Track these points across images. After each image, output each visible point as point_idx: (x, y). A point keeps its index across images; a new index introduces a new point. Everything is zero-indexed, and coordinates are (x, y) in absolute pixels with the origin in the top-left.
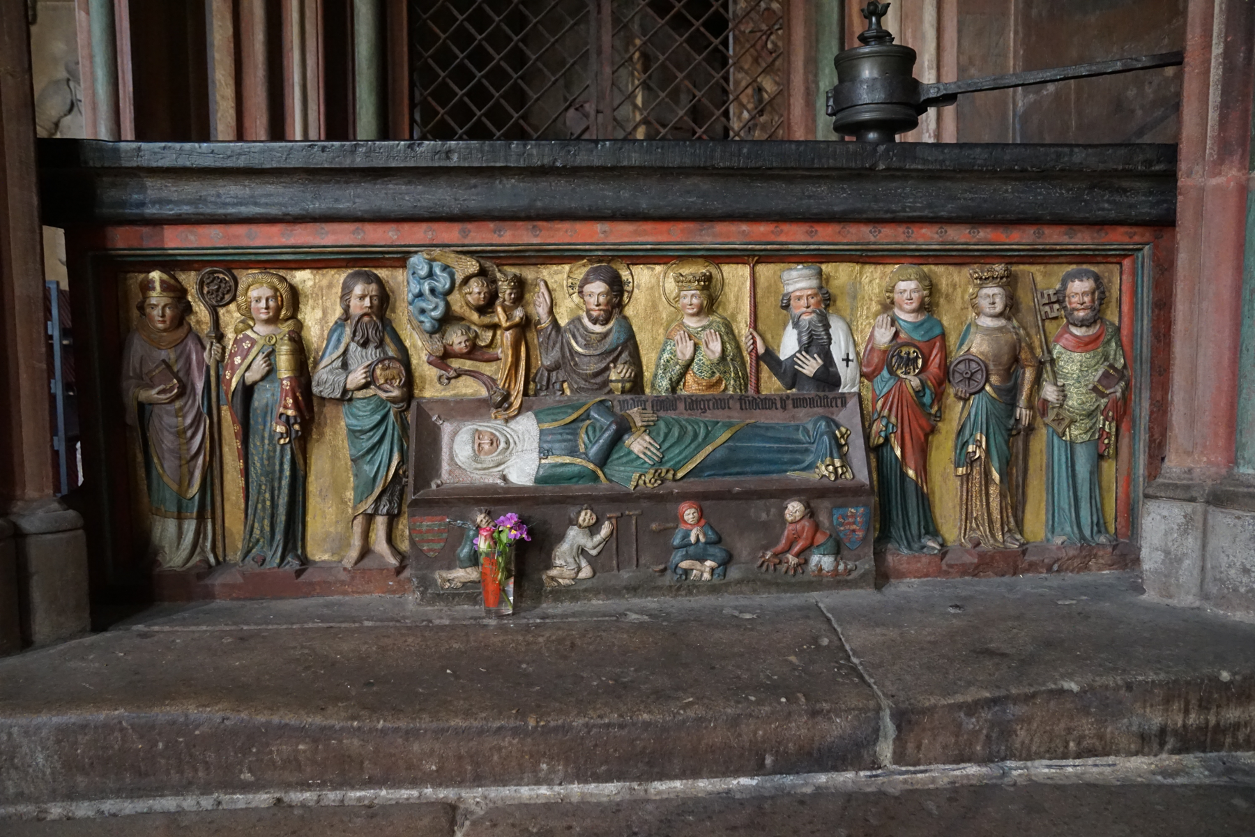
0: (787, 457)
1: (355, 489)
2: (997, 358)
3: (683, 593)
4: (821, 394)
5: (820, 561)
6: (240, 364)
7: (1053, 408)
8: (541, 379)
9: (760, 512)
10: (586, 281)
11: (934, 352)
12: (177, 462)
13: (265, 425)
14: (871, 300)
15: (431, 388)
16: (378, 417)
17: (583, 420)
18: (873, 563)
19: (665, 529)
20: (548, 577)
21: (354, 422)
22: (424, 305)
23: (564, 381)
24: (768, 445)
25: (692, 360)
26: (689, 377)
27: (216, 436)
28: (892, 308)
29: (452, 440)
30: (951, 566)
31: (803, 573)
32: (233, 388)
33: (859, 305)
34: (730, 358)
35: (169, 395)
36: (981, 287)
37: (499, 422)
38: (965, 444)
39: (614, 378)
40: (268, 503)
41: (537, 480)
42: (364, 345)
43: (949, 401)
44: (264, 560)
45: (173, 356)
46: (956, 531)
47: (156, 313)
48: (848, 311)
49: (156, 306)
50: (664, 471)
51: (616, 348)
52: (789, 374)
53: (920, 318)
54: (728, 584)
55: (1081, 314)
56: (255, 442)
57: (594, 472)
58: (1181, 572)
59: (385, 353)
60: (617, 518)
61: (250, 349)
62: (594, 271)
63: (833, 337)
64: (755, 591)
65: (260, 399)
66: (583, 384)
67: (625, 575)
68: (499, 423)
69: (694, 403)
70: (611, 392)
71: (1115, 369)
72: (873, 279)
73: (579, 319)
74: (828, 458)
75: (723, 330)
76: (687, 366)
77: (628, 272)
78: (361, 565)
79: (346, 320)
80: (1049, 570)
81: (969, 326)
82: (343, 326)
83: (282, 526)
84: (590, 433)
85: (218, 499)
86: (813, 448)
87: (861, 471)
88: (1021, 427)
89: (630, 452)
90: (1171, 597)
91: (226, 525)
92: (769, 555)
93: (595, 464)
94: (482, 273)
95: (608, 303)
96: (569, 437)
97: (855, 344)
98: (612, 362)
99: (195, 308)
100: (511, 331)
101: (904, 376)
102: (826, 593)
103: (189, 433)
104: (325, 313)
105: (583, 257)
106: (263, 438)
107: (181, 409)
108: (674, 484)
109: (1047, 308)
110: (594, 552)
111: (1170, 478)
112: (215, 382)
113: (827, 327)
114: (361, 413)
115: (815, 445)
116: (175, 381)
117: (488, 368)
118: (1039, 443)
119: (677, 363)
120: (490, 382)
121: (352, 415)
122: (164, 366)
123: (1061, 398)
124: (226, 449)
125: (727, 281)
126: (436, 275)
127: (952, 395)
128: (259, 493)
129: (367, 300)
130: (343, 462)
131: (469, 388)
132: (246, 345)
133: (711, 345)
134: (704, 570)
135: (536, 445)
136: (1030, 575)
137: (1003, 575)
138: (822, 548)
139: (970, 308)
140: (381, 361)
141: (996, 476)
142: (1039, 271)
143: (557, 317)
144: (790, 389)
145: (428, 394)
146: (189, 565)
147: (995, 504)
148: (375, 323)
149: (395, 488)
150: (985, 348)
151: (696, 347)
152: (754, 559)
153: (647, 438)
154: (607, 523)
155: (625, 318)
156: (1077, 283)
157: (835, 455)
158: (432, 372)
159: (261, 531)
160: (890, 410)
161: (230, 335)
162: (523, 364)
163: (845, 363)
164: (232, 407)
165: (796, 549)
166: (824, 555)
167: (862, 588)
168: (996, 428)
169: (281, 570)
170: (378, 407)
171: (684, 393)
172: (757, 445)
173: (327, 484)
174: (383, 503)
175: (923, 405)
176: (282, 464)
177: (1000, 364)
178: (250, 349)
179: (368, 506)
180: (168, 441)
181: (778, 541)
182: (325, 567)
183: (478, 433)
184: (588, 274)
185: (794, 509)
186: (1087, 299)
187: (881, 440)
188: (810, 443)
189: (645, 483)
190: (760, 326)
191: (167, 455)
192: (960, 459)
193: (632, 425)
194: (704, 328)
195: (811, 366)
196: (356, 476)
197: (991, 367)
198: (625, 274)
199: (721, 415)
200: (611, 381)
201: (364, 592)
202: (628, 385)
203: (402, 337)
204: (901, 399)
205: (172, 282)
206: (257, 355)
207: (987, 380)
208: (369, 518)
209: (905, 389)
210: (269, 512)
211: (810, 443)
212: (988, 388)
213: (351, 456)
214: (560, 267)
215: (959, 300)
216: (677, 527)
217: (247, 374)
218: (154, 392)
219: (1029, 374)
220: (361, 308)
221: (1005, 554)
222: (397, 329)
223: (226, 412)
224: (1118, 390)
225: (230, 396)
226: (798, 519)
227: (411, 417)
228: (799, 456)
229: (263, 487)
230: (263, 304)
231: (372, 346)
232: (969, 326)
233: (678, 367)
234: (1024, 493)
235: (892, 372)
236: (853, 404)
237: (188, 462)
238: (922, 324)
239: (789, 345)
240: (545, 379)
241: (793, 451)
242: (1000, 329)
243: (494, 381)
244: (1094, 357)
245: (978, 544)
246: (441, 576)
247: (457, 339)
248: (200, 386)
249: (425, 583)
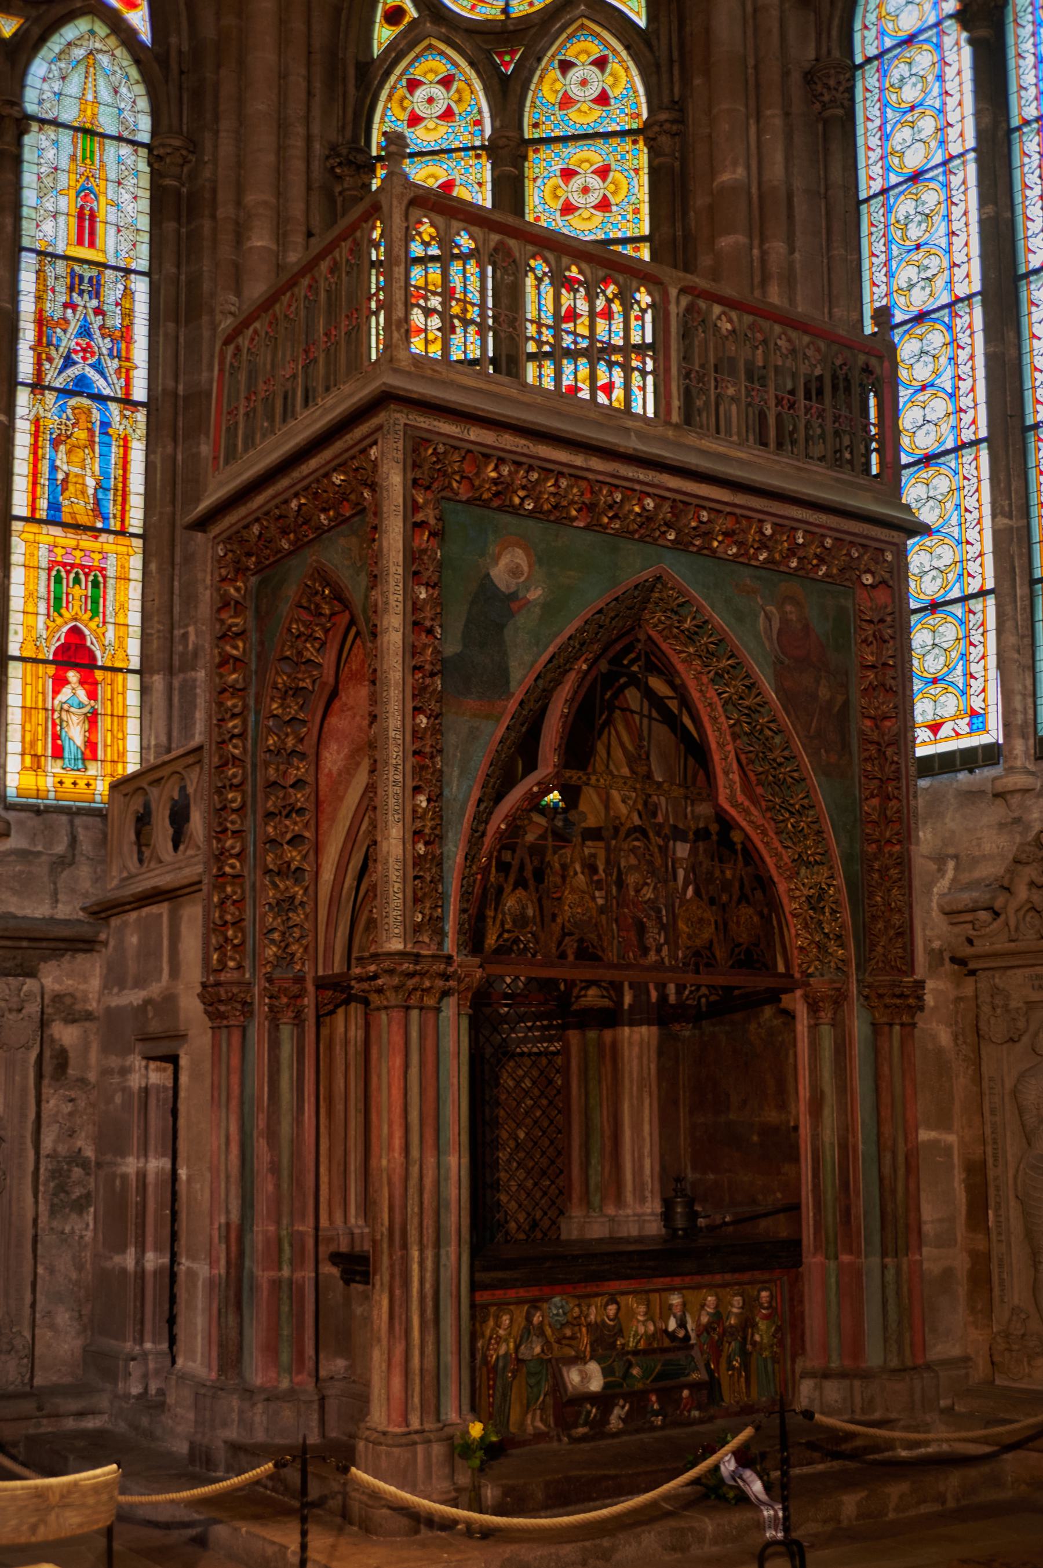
10: (607, 1304)
52: (672, 1336)
134: (659, 1420)
158: (556, 1346)
185: (686, 1393)
239: (672, 1325)
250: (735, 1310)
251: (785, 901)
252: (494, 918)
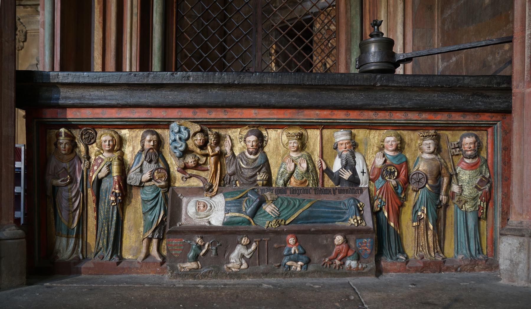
0: (335, 215)
1: (144, 227)
2: (431, 172)
3: (288, 276)
4: (351, 188)
5: (350, 263)
6: (97, 170)
7: (457, 195)
8: (227, 179)
9: (323, 240)
10: (247, 136)
11: (403, 169)
12: (68, 213)
13: (106, 197)
14: (374, 146)
16: (155, 194)
17: (245, 197)
18: (374, 265)
19: (281, 247)
20: (228, 267)
21: (144, 196)
22: (176, 145)
23: (237, 180)
24: (327, 210)
25: (294, 171)
26: (292, 179)
27: (85, 201)
28: (383, 150)
29: (187, 205)
30: (410, 268)
31: (343, 268)
32: (93, 180)
33: (369, 148)
34: (310, 170)
35: (65, 183)
36: (423, 140)
37: (207, 198)
38: (417, 211)
39: (259, 179)
40: (106, 232)
41: (224, 224)
42: (150, 162)
43: (409, 192)
44: (103, 257)
45: (68, 165)
46: (413, 252)
47: (62, 146)
48: (364, 151)
49: (62, 143)
50: (280, 220)
51: (260, 166)
52: (337, 179)
53: (396, 154)
54: (308, 273)
55: (469, 153)
56: (101, 204)
57: (249, 220)
58: (518, 270)
59: (159, 166)
60: (259, 241)
61: (101, 163)
62: (251, 131)
63: (357, 162)
64: (321, 276)
65: (105, 185)
66: (245, 181)
67: (262, 267)
68: (207, 198)
69: (294, 191)
70: (257, 185)
71: (485, 178)
73: (244, 153)
74: (354, 216)
75: (307, 158)
76: (292, 174)
77: (266, 132)
78: (145, 261)
79: (143, 151)
80: (456, 270)
81: (418, 158)
82: (141, 154)
83: (112, 242)
84: (248, 203)
85: (85, 230)
86: (347, 212)
87: (369, 222)
88: (442, 204)
89: (265, 212)
90: (514, 282)
91: (88, 241)
92: (327, 260)
93: (249, 217)
94: (202, 131)
95: (257, 145)
96: (238, 204)
97: (367, 166)
98: (258, 172)
99: (79, 145)
100: (214, 157)
101: (389, 180)
102: (353, 278)
103: (74, 200)
104: (134, 148)
105: (245, 125)
106: (105, 203)
107: (71, 189)
108: (285, 226)
109: (454, 150)
110: (248, 257)
111: (512, 226)
112: (85, 177)
113: (354, 157)
114: (148, 193)
115: (348, 211)
116: (68, 176)
117: (203, 174)
118: (451, 212)
119: (287, 173)
120: (204, 180)
121: (143, 193)
122: (64, 170)
123: (461, 191)
124: (89, 207)
125: (309, 137)
126: (182, 132)
127: (411, 189)
128: (102, 227)
129: (152, 142)
130: (139, 215)
131: (195, 182)
132: (99, 161)
133: (302, 165)
134: (298, 266)
135: (223, 208)
136: (447, 273)
137: (434, 272)
138: (351, 257)
139: (419, 150)
140: (157, 169)
141: (431, 226)
142: (450, 133)
143: (234, 152)
144: (338, 185)
145: (177, 185)
146: (71, 258)
147: (431, 239)
148: (155, 152)
150: (425, 168)
151: (296, 166)
152: (320, 262)
153: (273, 205)
154: (254, 243)
155: (264, 152)
156: (467, 138)
157: (357, 214)
158: (179, 175)
159: (103, 244)
160: (383, 195)
161: (93, 157)
162: (219, 172)
163: (362, 174)
165: (340, 257)
166: (352, 260)
167: (369, 276)
168: (431, 204)
169: (111, 262)
170: (155, 190)
171: (290, 186)
172: (322, 210)
173: (132, 224)
174: (156, 233)
175: (398, 193)
176: (112, 214)
177: (433, 175)
178: (101, 163)
179: (149, 234)
180: (64, 203)
181: (331, 253)
182: (131, 262)
183: (198, 202)
184: (248, 133)
185: (339, 239)
186: (472, 146)
187: (379, 209)
188: (346, 209)
189: (271, 226)
190: (324, 157)
191: (63, 209)
192: (414, 218)
193: (266, 199)
194: (299, 157)
195: (347, 175)
196: (144, 220)
197: (429, 176)
198: (264, 133)
199: (306, 196)
200: (258, 180)
201: (147, 273)
202: (265, 182)
203: (167, 160)
204: (387, 191)
205: (69, 133)
206: (104, 166)
207: (427, 182)
208: (150, 240)
209: (389, 185)
210: (106, 235)
211: (346, 209)
212: (427, 186)
213: (143, 211)
214: (236, 130)
215: (414, 146)
216: (285, 247)
217: (99, 174)
218: (59, 181)
219: (446, 180)
220: (149, 146)
221: (436, 263)
222: (165, 156)
223: (90, 191)
224: (487, 188)
225: (91, 184)
226: (340, 243)
227: (169, 195)
228: (341, 216)
229: (104, 224)
230: (107, 143)
231: (153, 162)
232: (418, 158)
233: (287, 174)
235: (383, 178)
236: (366, 192)
237: (72, 212)
238: (397, 156)
239: (337, 166)
240: (228, 179)
241: (339, 213)
242: (432, 159)
243: (206, 179)
244: (476, 172)
245: (423, 258)
246: (180, 266)
248: (79, 179)
249: (173, 268)
250: (426, 156)
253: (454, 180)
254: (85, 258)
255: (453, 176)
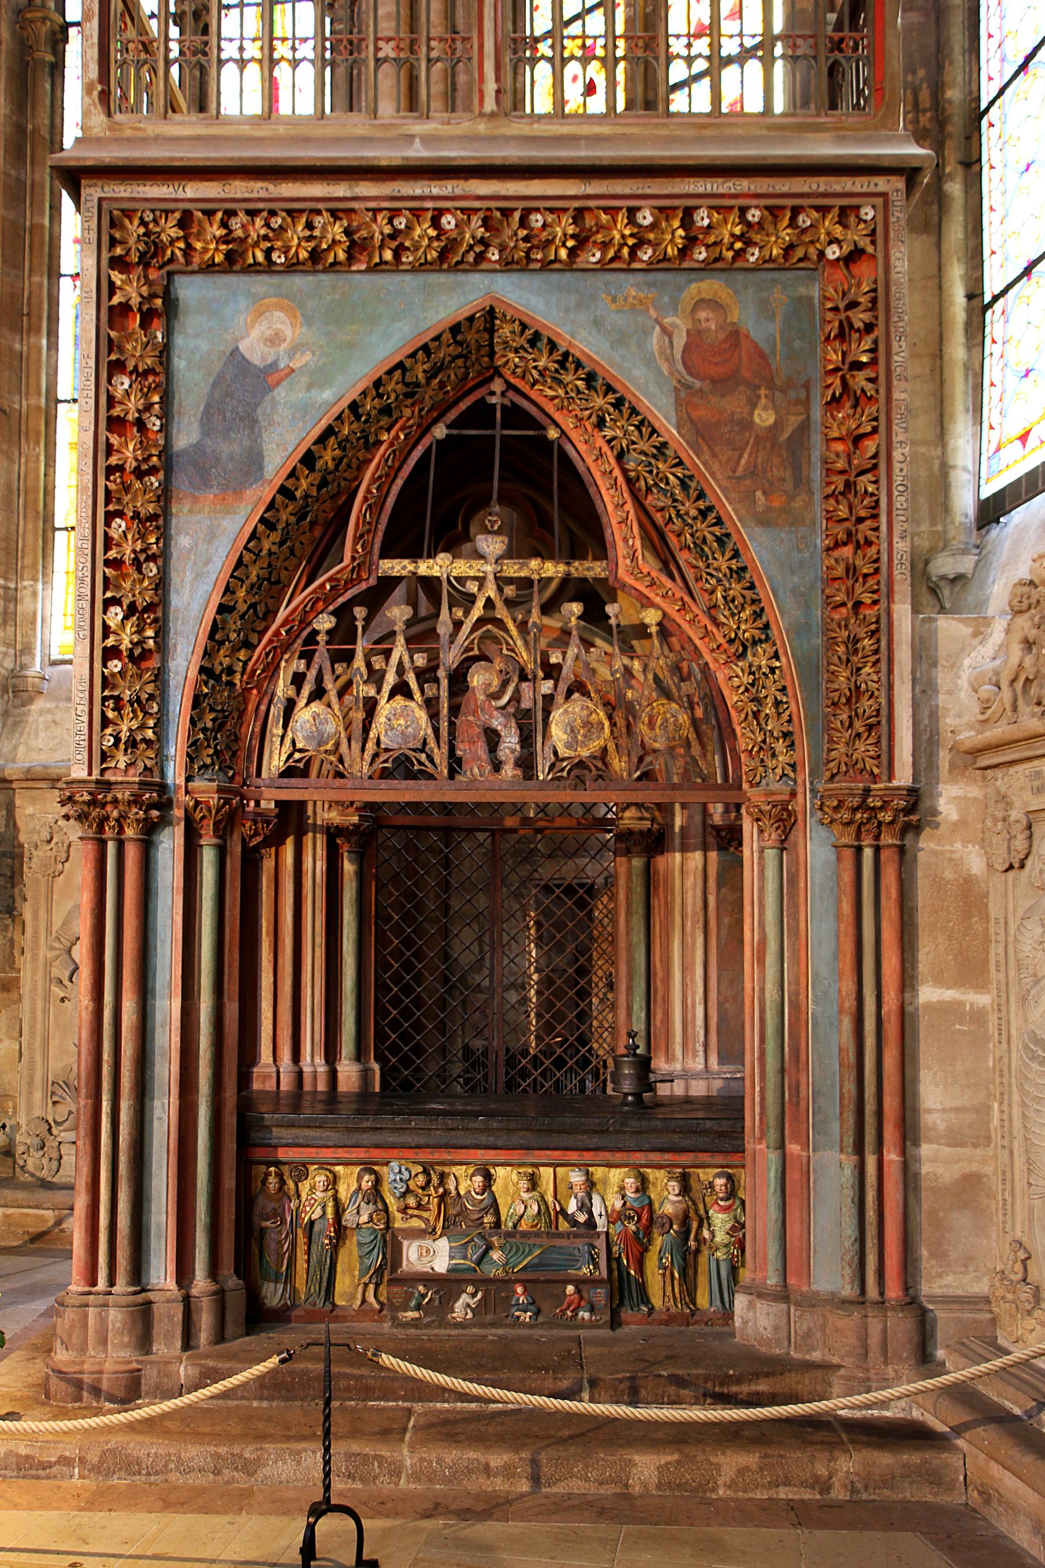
2: (676, 1216)
10: (473, 1175)
15: (399, 1222)
47: (271, 1186)
56: (314, 1248)
65: (317, 1228)
67: (489, 1317)
68: (430, 1242)
69: (524, 1234)
72: (615, 1175)
80: (706, 1324)
113: (590, 1199)
118: (703, 1259)
131: (416, 1223)
141: (676, 1275)
145: (396, 1225)
147: (677, 1290)
149: (379, 1271)
158: (399, 1215)
164: (304, 1231)
179: (366, 1279)
180: (273, 1246)
185: (570, 1289)
195: (582, 1218)
198: (492, 1171)
199: (538, 1241)
207: (671, 1227)
208: (366, 1285)
218: (268, 1223)
219: (695, 1225)
221: (682, 1315)
223: (300, 1232)
227: (388, 1237)
234: (695, 1284)
236: (603, 1237)
242: (679, 1202)
247: (411, 1201)
251: (726, 692)
252: (283, 737)
253: (705, 1224)
254: (294, 1306)
255: (704, 1220)
